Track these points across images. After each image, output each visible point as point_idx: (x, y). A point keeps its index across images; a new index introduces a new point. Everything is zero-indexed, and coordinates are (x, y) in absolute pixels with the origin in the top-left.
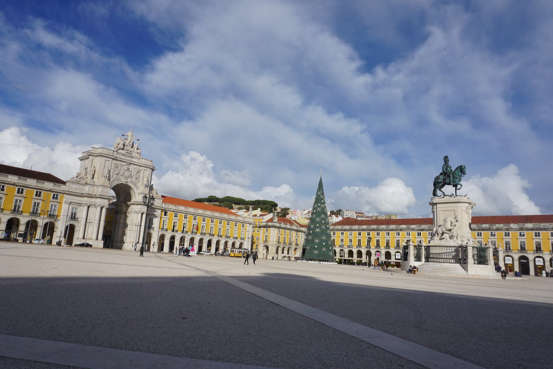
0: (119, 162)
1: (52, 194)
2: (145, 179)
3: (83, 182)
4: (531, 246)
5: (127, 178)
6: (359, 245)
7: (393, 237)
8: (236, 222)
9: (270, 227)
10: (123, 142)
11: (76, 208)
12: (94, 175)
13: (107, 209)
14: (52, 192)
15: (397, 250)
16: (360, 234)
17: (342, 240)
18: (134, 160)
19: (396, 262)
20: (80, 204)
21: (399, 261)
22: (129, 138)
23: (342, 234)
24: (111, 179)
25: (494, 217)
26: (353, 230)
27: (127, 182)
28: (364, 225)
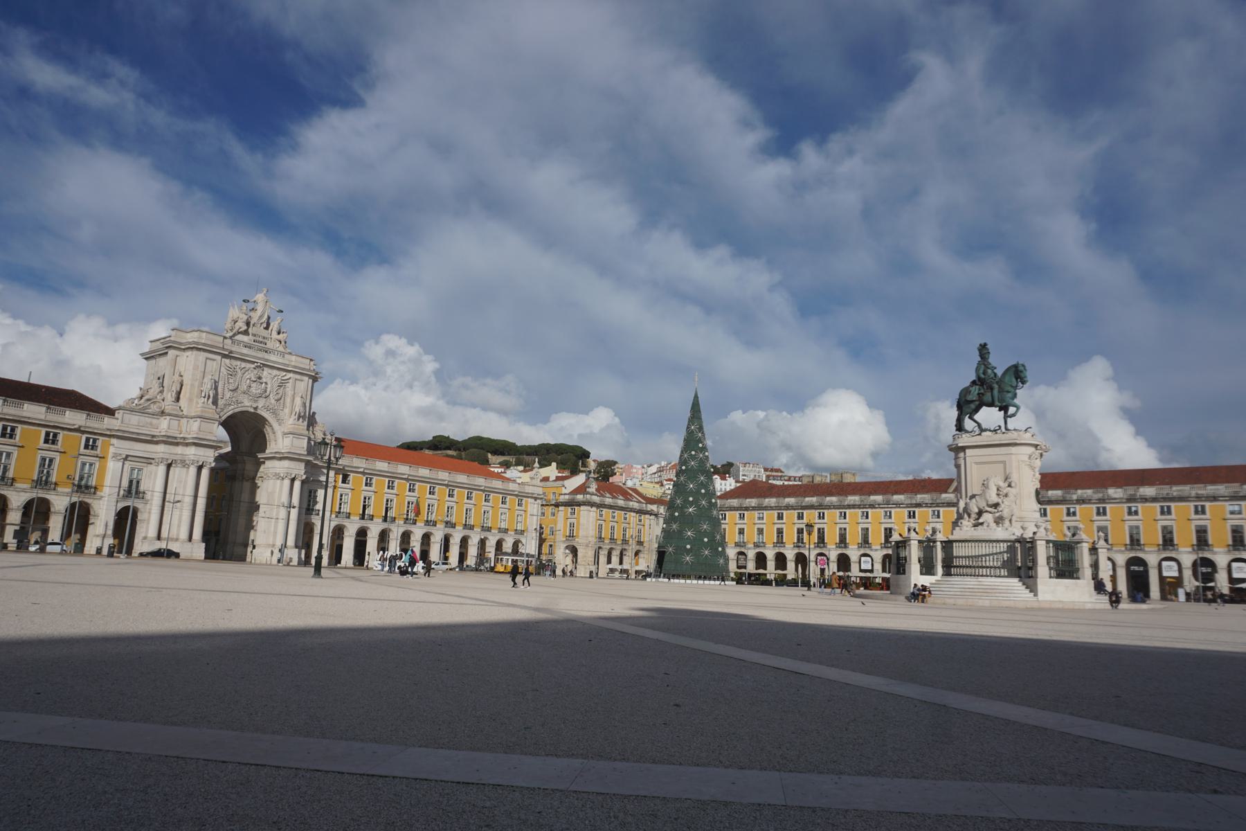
0: (238, 363)
1: (84, 437)
2: (298, 401)
4: (1152, 537)
5: (257, 397)
6: (780, 541)
7: (854, 523)
8: (505, 494)
10: (245, 318)
11: (140, 470)
12: (179, 393)
13: (212, 470)
14: (84, 432)
15: (862, 551)
16: (780, 517)
17: (741, 532)
18: (273, 357)
19: (861, 578)
20: (149, 461)
21: (868, 575)
22: (260, 308)
24: (221, 402)
25: (1073, 473)
26: (766, 508)
27: (256, 408)
28: (789, 496)
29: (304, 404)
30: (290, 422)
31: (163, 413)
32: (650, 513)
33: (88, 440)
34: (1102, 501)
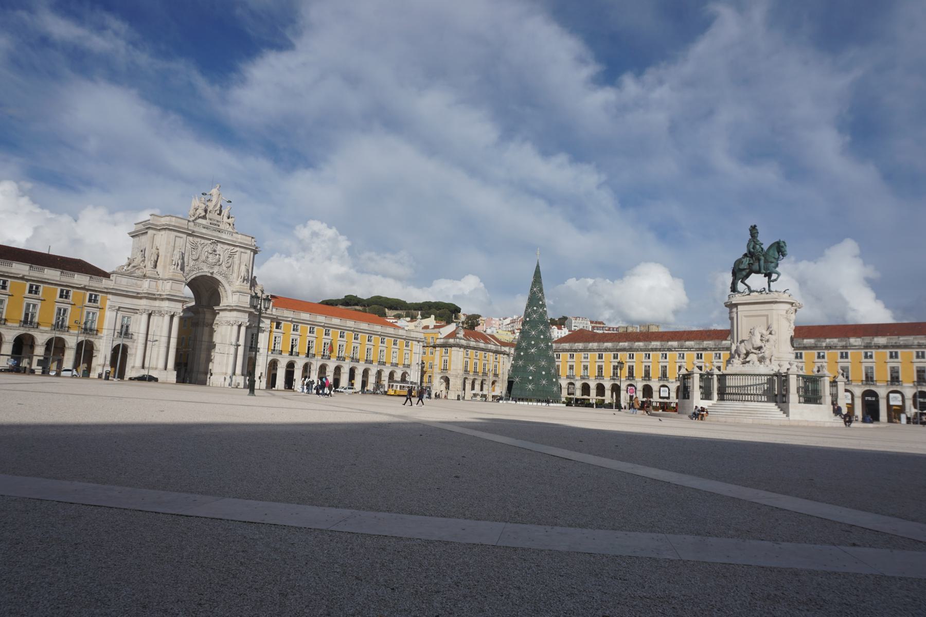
0: (199, 240)
1: (88, 294)
2: (243, 268)
3: (138, 273)
4: (882, 374)
5: (213, 266)
6: (600, 375)
7: (656, 362)
8: (396, 338)
9: (451, 346)
10: (204, 206)
11: (129, 318)
12: (156, 262)
13: (181, 318)
14: (88, 290)
15: (662, 383)
16: (600, 357)
17: (571, 367)
18: (224, 236)
19: (660, 403)
20: (135, 311)
21: (666, 400)
22: (214, 199)
23: (572, 356)
24: (186, 269)
25: (824, 327)
26: (590, 350)
27: (212, 273)
28: (607, 341)
29: (248, 271)
30: (238, 284)
31: (145, 276)
32: (504, 353)
33: (91, 295)
34: (845, 347)
